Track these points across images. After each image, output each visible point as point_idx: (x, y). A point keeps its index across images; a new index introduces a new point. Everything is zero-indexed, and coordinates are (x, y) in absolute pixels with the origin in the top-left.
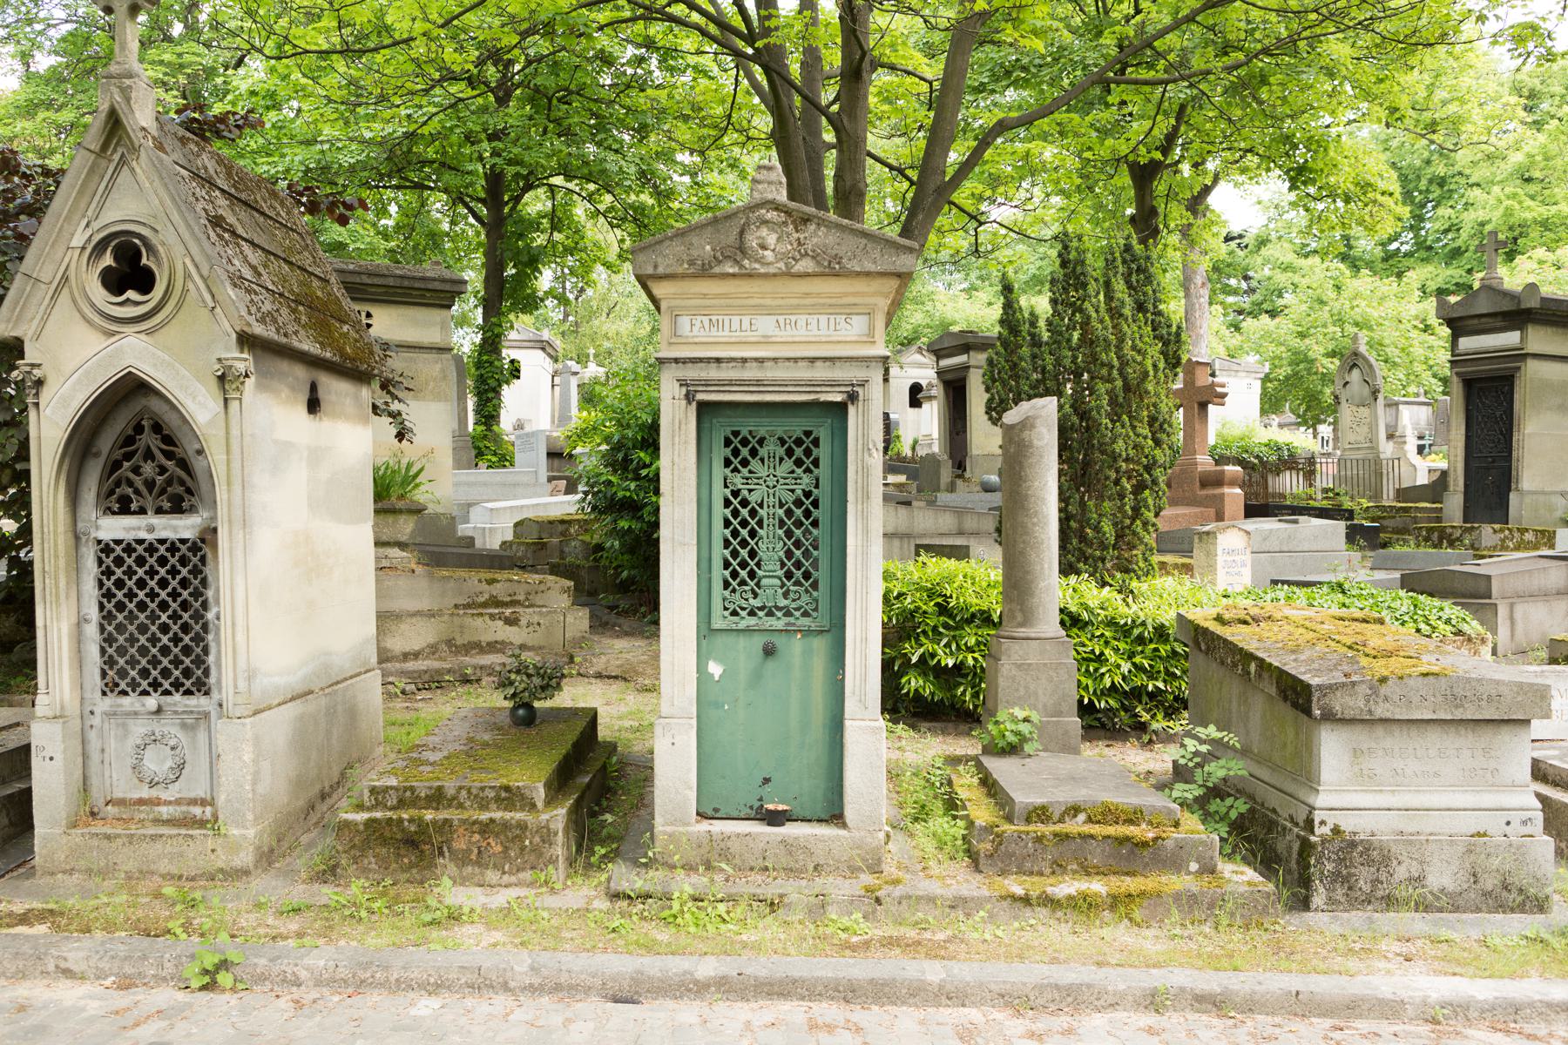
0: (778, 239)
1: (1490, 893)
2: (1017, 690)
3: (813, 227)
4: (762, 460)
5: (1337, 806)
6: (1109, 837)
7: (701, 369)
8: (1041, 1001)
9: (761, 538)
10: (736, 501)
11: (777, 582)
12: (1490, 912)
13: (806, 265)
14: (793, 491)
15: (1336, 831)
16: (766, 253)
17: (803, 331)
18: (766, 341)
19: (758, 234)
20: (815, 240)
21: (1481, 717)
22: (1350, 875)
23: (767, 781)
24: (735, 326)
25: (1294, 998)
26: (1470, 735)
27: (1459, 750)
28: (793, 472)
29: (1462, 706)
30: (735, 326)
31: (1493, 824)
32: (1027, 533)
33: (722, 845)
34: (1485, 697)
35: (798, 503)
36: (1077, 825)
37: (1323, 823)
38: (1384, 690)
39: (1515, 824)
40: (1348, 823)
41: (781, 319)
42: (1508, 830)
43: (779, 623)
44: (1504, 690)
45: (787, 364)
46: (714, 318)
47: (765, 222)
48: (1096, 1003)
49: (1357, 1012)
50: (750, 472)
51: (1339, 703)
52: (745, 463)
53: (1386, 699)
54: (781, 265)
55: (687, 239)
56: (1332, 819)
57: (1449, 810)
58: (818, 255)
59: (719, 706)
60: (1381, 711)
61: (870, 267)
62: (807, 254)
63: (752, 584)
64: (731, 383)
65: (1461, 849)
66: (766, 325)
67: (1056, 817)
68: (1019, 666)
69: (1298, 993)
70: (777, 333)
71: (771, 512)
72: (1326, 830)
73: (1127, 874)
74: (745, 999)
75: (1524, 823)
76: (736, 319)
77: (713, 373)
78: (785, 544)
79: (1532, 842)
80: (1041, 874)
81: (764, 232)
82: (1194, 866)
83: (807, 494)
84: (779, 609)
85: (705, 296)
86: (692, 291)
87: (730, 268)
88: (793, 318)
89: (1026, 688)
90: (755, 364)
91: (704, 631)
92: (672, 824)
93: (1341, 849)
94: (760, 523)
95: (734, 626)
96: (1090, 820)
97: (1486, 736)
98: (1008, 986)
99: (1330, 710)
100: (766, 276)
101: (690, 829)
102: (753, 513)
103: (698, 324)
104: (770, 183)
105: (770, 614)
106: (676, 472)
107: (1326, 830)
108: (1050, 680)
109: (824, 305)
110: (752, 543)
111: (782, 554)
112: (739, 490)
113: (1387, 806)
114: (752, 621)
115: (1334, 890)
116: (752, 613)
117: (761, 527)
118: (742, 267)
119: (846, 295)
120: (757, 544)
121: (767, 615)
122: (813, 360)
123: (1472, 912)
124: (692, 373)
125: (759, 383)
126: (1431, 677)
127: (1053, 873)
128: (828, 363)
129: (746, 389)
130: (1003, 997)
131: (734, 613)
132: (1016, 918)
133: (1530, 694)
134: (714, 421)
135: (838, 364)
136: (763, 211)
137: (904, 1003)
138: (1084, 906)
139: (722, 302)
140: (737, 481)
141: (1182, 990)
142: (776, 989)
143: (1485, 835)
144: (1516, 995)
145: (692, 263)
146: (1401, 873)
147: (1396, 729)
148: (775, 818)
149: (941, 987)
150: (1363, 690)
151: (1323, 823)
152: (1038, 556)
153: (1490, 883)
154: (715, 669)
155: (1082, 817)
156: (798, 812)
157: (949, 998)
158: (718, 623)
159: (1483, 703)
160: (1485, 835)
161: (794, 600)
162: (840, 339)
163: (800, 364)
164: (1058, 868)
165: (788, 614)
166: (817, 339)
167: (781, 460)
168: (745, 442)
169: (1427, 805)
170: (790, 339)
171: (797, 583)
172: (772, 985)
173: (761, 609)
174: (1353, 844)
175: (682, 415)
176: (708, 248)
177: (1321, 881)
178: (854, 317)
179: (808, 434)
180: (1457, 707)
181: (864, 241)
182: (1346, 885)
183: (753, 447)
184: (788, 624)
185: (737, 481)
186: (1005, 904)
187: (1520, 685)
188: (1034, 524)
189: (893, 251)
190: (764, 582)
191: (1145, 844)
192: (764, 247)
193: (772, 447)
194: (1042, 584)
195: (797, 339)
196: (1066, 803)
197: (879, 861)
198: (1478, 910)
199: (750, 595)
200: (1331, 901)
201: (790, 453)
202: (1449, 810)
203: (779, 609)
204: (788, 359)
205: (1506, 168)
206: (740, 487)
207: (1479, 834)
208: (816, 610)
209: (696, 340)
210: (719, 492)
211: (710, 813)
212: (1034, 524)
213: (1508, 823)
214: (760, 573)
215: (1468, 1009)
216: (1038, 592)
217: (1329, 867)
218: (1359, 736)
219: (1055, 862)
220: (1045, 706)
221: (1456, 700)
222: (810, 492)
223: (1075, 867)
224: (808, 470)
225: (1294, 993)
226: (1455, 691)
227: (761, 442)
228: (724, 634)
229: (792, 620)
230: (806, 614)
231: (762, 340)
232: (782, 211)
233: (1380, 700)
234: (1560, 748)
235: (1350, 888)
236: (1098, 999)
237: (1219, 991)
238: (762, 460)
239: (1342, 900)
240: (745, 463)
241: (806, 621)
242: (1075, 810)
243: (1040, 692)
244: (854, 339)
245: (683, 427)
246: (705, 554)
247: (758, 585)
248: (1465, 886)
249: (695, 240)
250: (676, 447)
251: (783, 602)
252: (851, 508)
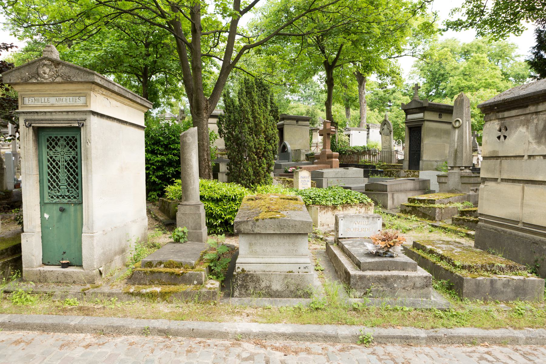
0: (50, 71)
1: (293, 291)
2: (182, 222)
3: (61, 66)
4: (59, 146)
5: (243, 262)
6: (167, 272)
7: (32, 115)
8: (107, 332)
10: (52, 161)
11: (66, 187)
12: (293, 298)
13: (59, 79)
14: (69, 157)
15: (243, 270)
16: (45, 75)
17: (65, 103)
18: (52, 106)
19: (43, 69)
20: (62, 71)
21: (289, 233)
22: (247, 285)
23: (64, 253)
24: (43, 101)
25: (192, 331)
26: (288, 238)
27: (283, 244)
28: (69, 150)
29: (283, 229)
30: (43, 101)
31: (294, 268)
32: (185, 171)
33: (44, 275)
34: (291, 226)
35: (71, 161)
36: (161, 269)
37: (238, 268)
38: (257, 223)
39: (302, 268)
40: (247, 268)
41: (57, 98)
42: (300, 270)
43: (66, 201)
44: (297, 223)
45: (59, 113)
46: (36, 98)
47: (45, 65)
48: (126, 332)
49: (212, 336)
50: (56, 150)
51: (243, 228)
52: (54, 147)
53: (258, 226)
54: (51, 79)
55: (20, 71)
56: (242, 267)
57: (280, 263)
58: (63, 76)
59: (48, 228)
60: (257, 230)
61: (80, 80)
62: (59, 76)
64: (42, 120)
65: (283, 277)
66: (53, 100)
67: (154, 265)
68: (183, 214)
69: (193, 329)
70: (56, 103)
72: (240, 270)
73: (174, 285)
74: (10, 330)
75: (305, 268)
76: (43, 98)
77: (36, 117)
79: (306, 274)
80: (146, 284)
81: (45, 68)
82: (195, 282)
83: (74, 158)
84: (66, 196)
85: (32, 91)
86: (27, 89)
87: (34, 81)
88: (61, 98)
89: (185, 221)
90: (49, 114)
91: (42, 204)
92: (28, 267)
93: (243, 277)
94: (59, 167)
95: (51, 202)
96: (165, 267)
97: (293, 239)
98: (97, 326)
99: (240, 230)
100: (47, 83)
101: (34, 269)
102: (57, 164)
103: (31, 100)
104: (48, 51)
105: (63, 198)
106: (26, 150)
107: (240, 270)
108: (193, 218)
109: (70, 93)
111: (66, 178)
112: (52, 156)
113: (259, 262)
114: (57, 200)
115: (241, 290)
116: (58, 197)
118: (38, 80)
119: (77, 90)
122: (68, 112)
123: (287, 298)
124: (29, 117)
125: (51, 120)
126: (273, 219)
127: (150, 284)
128: (73, 113)
129: (47, 122)
130: (95, 330)
131: (52, 197)
132: (128, 300)
133: (306, 225)
135: (76, 113)
136: (44, 61)
137: (62, 332)
138: (152, 296)
139: (38, 92)
140: (51, 153)
141: (154, 328)
142: (20, 327)
143: (292, 272)
144: (267, 330)
145: (22, 79)
146: (263, 285)
147: (263, 236)
148: (65, 266)
149: (75, 326)
150: (251, 223)
151: (238, 268)
152: (189, 178)
153: (292, 288)
154: (46, 216)
155: (162, 265)
156: (74, 263)
157: (78, 330)
158: (46, 201)
159: (290, 228)
160: (292, 272)
161: (71, 193)
162: (76, 105)
163: (64, 113)
164: (151, 283)
165: (69, 198)
166: (69, 105)
167: (65, 146)
168: (53, 140)
169: (273, 262)
170: (60, 105)
171: (72, 187)
172: (19, 325)
173: (61, 196)
174: (247, 275)
175: (27, 131)
176: (27, 74)
177: (237, 287)
178: (81, 97)
179: (73, 137)
180: (282, 229)
181: (78, 71)
182: (245, 289)
183: (56, 142)
184: (68, 201)
185: (51, 153)
186: (126, 295)
187: (302, 222)
188: (188, 168)
189: (87, 74)
190: (61, 187)
191: (179, 275)
192: (45, 73)
193: (62, 142)
194: (191, 187)
195: (62, 105)
196: (157, 261)
197: (94, 280)
198: (289, 297)
199: (57, 191)
200: (240, 294)
201: (68, 144)
202: (280, 263)
203: (66, 196)
204: (59, 112)
207: (290, 272)
208: (78, 196)
209: (30, 106)
210: (45, 157)
211: (47, 263)
212: (188, 168)
213: (300, 268)
214: (60, 184)
215: (250, 335)
216: (189, 190)
217: (240, 283)
218: (251, 239)
219: (150, 281)
220: (191, 227)
221: (281, 227)
222: (75, 157)
223: (157, 282)
224: (74, 150)
225: (192, 329)
226: (281, 224)
227: (59, 140)
228: (49, 204)
229: (70, 200)
230: (75, 198)
231: (51, 105)
232: (50, 61)
233: (256, 227)
234: (353, 240)
235: (247, 290)
236: (126, 331)
237: (166, 328)
238: (59, 146)
239: (244, 294)
240: (54, 147)
241: (75, 200)
242: (160, 263)
243: (190, 222)
244: (82, 105)
245: (28, 135)
246: (41, 178)
247: (59, 188)
248: (285, 289)
249: (23, 71)
250: (26, 142)
251: (68, 194)
252: (83, 162)
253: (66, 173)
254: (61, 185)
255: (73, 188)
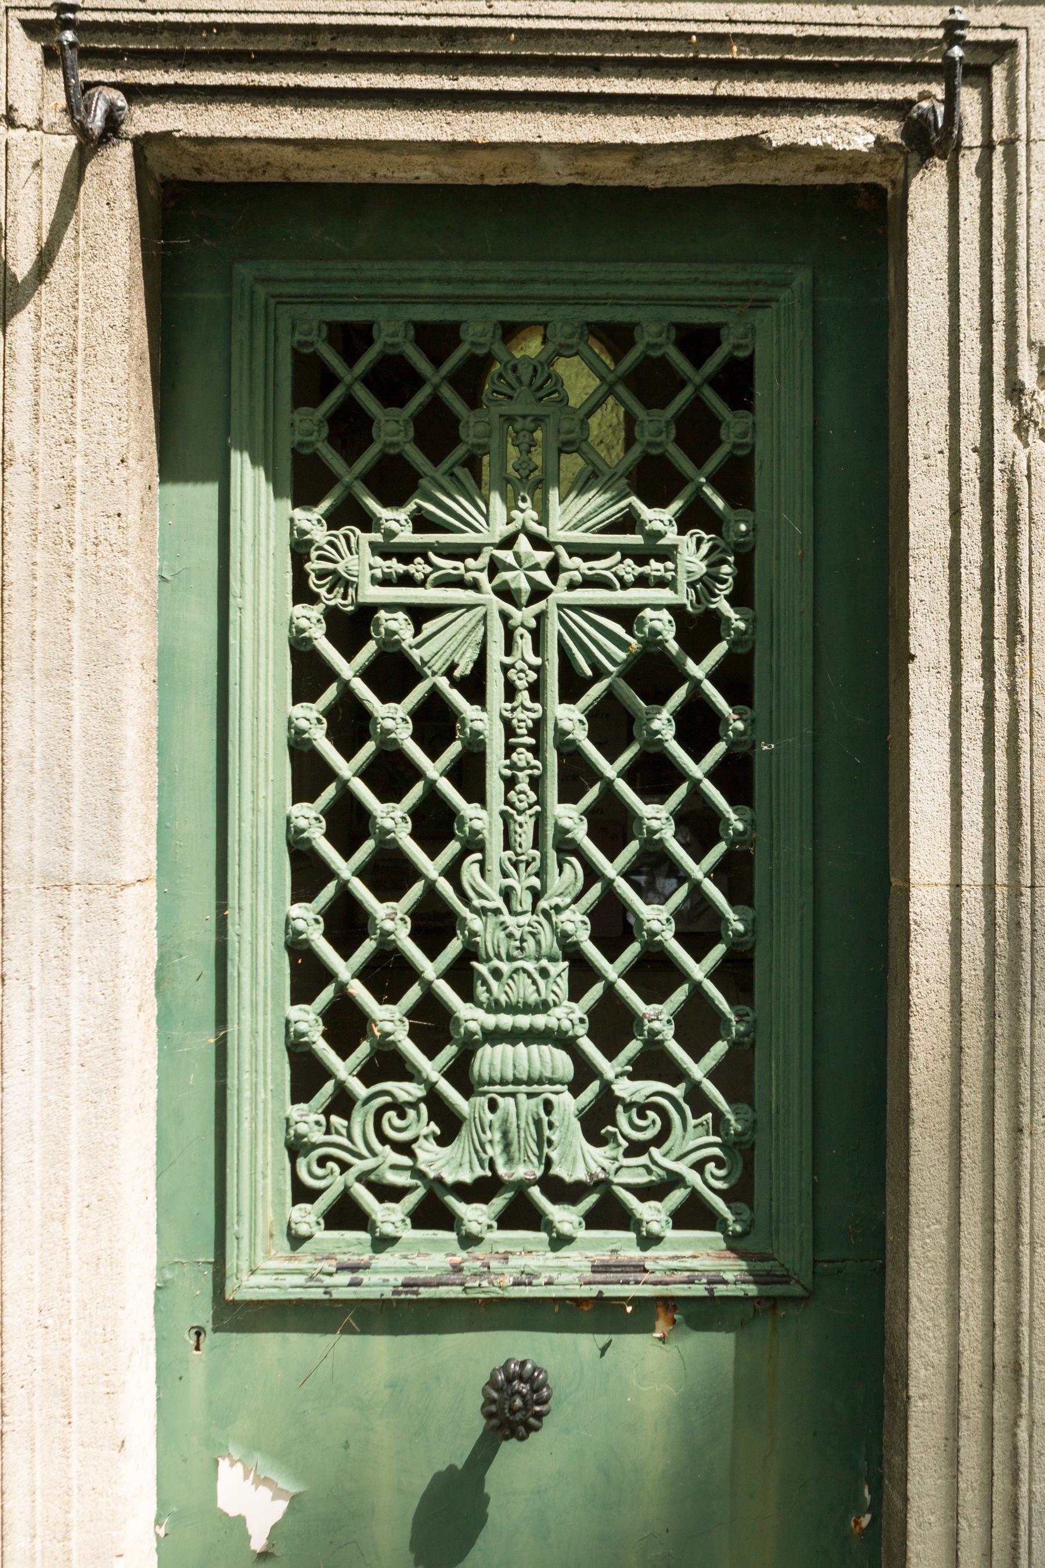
9: (474, 844)
11: (563, 1063)
63: (431, 1068)
71: (524, 719)
78: (592, 874)
95: (341, 1286)
110: (431, 868)
112: (367, 612)
117: (476, 794)
120: (452, 872)
121: (506, 1221)
134: (244, 271)
161: (636, 1149)
183: (436, 405)
206: (372, 594)
253: (567, 847)
254: (494, 1036)
255: (674, 1074)
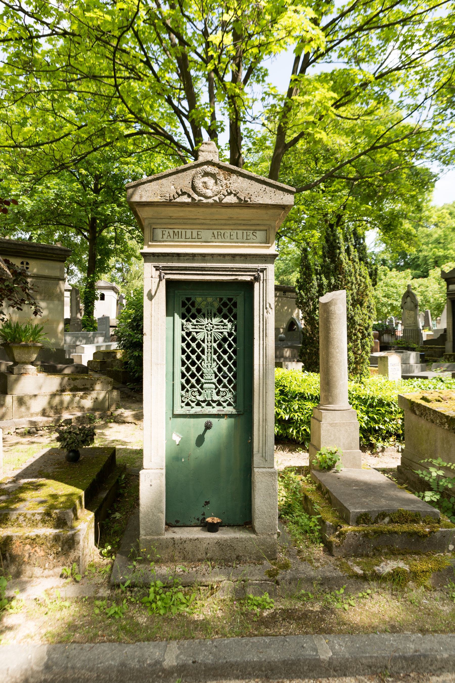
6: (405, 532)
8: (395, 669)
9: (203, 360)
11: (214, 386)
20: (236, 185)
24: (189, 235)
33: (181, 546)
41: (215, 232)
46: (176, 231)
63: (198, 387)
67: (373, 520)
68: (331, 425)
71: (209, 345)
73: (415, 553)
76: (189, 232)
78: (217, 364)
80: (367, 556)
84: (214, 402)
88: (223, 232)
90: (200, 258)
92: (150, 534)
94: (203, 352)
96: (391, 521)
98: (374, 660)
101: (162, 537)
102: (199, 346)
103: (166, 234)
104: (210, 152)
105: (209, 404)
110: (198, 363)
111: (216, 370)
112: (191, 332)
116: (198, 404)
117: (203, 354)
120: (201, 363)
121: (207, 405)
128: (243, 258)
131: (188, 404)
134: (176, 292)
142: (219, 672)
155: (387, 520)
157: (335, 671)
161: (223, 396)
165: (219, 404)
171: (225, 386)
172: (215, 669)
173: (204, 401)
178: (258, 232)
179: (230, 300)
181: (264, 186)
185: (189, 326)
186: (352, 580)
190: (205, 386)
191: (425, 536)
196: (378, 511)
199: (197, 394)
205: (432, 239)
206: (191, 330)
210: (179, 333)
211: (174, 523)
214: (203, 381)
220: (344, 444)
223: (386, 551)
229: (221, 408)
242: (383, 515)
247: (202, 388)
251: (216, 398)
253: (214, 360)
254: (206, 383)
255: (227, 388)
